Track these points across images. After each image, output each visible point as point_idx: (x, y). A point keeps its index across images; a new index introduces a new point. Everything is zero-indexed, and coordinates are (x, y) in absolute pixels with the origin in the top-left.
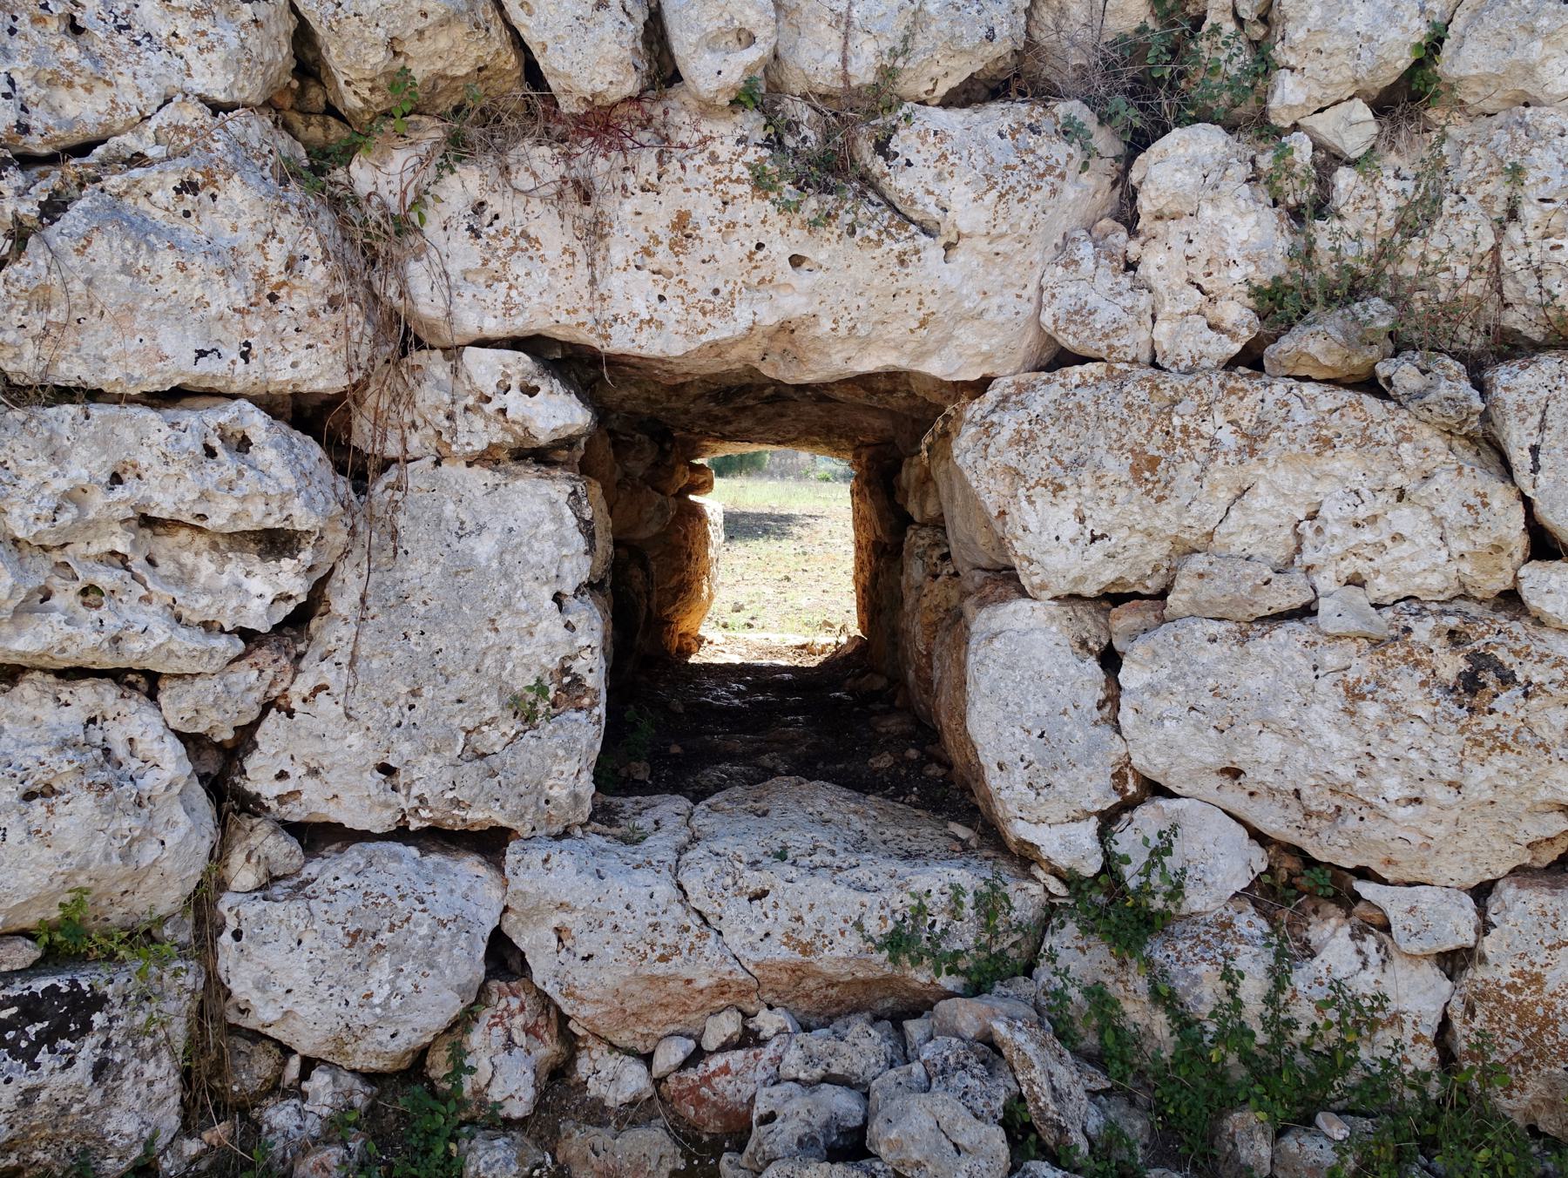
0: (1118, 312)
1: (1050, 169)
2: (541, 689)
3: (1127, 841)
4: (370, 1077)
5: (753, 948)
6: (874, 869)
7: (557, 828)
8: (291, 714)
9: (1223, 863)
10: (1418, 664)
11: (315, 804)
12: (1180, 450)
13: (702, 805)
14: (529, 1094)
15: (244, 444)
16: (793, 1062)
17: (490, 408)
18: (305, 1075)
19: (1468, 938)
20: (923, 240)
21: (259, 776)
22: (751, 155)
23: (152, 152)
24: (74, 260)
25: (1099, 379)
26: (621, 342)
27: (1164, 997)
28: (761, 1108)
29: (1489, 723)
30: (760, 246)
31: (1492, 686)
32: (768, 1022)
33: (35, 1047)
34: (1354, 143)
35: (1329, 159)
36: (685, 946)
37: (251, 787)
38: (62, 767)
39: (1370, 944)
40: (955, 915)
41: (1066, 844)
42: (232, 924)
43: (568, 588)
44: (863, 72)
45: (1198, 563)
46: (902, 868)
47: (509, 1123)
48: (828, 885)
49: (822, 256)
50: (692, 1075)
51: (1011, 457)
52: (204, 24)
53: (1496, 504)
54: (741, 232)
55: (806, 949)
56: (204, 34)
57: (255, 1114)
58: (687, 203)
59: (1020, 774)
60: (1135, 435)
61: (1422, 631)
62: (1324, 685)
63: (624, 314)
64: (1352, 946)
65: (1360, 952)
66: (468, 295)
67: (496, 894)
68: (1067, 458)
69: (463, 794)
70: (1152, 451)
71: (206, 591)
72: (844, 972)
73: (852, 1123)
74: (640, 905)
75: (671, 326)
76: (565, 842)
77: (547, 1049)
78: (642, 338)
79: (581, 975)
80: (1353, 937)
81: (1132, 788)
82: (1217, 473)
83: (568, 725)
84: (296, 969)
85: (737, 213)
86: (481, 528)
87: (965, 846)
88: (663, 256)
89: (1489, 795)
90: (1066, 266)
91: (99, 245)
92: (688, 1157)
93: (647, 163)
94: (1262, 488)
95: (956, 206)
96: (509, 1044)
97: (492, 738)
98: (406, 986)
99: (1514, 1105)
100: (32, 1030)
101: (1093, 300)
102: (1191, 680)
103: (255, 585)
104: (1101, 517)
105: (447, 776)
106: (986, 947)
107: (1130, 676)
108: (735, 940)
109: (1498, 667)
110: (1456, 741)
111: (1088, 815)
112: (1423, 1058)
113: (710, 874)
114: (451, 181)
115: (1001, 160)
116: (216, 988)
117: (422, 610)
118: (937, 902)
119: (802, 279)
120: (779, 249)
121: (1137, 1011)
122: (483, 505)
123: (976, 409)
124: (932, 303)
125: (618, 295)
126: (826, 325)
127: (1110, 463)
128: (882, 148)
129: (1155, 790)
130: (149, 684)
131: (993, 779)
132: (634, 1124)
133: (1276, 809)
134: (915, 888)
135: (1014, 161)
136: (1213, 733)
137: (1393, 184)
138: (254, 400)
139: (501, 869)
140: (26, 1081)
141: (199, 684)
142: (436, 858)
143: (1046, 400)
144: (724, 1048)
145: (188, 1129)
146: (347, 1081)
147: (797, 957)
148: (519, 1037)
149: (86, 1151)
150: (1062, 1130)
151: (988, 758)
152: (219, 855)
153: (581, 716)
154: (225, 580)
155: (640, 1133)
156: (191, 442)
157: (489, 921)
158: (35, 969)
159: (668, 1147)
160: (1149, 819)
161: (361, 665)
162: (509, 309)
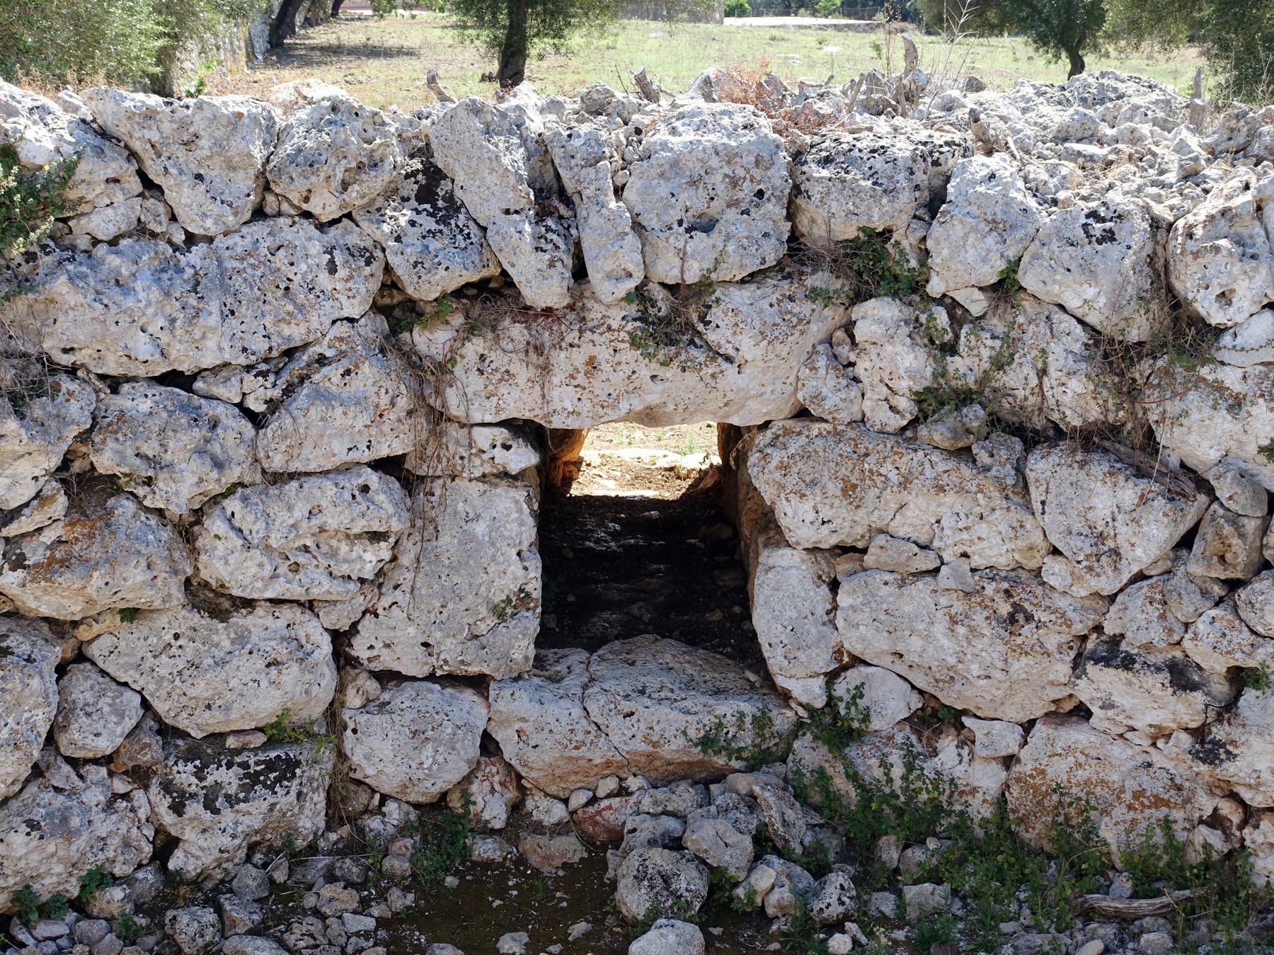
0: (838, 401)
1: (800, 321)
2: (508, 600)
3: (841, 689)
4: (417, 806)
5: (626, 743)
7: (515, 675)
8: (377, 616)
9: (892, 704)
10: (986, 607)
11: (388, 661)
12: (868, 482)
13: (595, 657)
14: (504, 817)
15: (365, 489)
16: (647, 804)
17: (485, 457)
19: (1014, 749)
20: (725, 365)
21: (359, 648)
22: (630, 327)
23: (329, 353)
24: (302, 420)
25: (829, 433)
27: (853, 777)
28: (629, 826)
29: (1019, 640)
30: (634, 372)
31: (1022, 622)
32: (633, 783)
33: (274, 784)
34: (976, 310)
36: (588, 741)
37: (354, 653)
38: (282, 652)
39: (965, 751)
40: (740, 727)
41: (805, 691)
42: (351, 725)
43: (525, 547)
44: (692, 277)
46: (711, 701)
47: (493, 832)
48: (668, 710)
49: (668, 375)
50: (591, 810)
52: (350, 285)
53: (1028, 526)
54: (624, 367)
55: (655, 745)
56: (350, 290)
57: (359, 822)
58: (594, 351)
59: (780, 651)
60: (843, 472)
61: (990, 589)
62: (940, 614)
63: (559, 409)
64: (956, 752)
65: (959, 755)
66: (477, 404)
67: (484, 711)
68: (808, 479)
69: (468, 658)
70: (854, 481)
71: (345, 561)
72: (677, 758)
73: (676, 835)
74: (564, 719)
75: (584, 414)
76: (521, 682)
77: (512, 794)
78: (569, 421)
79: (532, 756)
80: (957, 747)
81: (846, 659)
82: (887, 495)
83: (524, 621)
84: (384, 749)
86: (478, 517)
87: (752, 686)
88: (581, 379)
89: (1024, 676)
90: (811, 370)
91: (313, 411)
92: (590, 852)
93: (572, 337)
94: (912, 505)
95: (743, 348)
96: (493, 791)
97: (482, 628)
98: (440, 759)
100: (272, 776)
101: (825, 391)
102: (873, 605)
103: (368, 556)
104: (826, 513)
105: (459, 649)
106: (758, 746)
107: (843, 599)
108: (616, 739)
109: (1025, 611)
110: (1003, 648)
111: (819, 675)
112: (987, 812)
113: (602, 702)
114: (468, 344)
115: (770, 321)
116: (341, 755)
117: (447, 562)
118: (730, 720)
119: (659, 386)
121: (841, 783)
122: (478, 503)
123: (763, 439)
124: (731, 396)
125: (556, 400)
126: (671, 407)
127: (830, 485)
128: (702, 319)
129: (857, 661)
130: (310, 606)
132: (559, 834)
133: (922, 676)
134: (718, 713)
135: (778, 320)
136: (885, 634)
137: (989, 342)
139: (487, 698)
140: (271, 800)
141: (339, 606)
142: (449, 690)
143: (796, 446)
144: (608, 796)
145: (329, 828)
146: (406, 807)
147: (650, 749)
148: (497, 787)
149: (289, 835)
150: (786, 841)
151: (762, 640)
152: (341, 689)
153: (529, 614)
154: (354, 555)
155: (563, 838)
156: (347, 496)
157: (481, 725)
158: (265, 747)
159: (578, 846)
160: (853, 677)
161: (417, 592)
162: (498, 410)
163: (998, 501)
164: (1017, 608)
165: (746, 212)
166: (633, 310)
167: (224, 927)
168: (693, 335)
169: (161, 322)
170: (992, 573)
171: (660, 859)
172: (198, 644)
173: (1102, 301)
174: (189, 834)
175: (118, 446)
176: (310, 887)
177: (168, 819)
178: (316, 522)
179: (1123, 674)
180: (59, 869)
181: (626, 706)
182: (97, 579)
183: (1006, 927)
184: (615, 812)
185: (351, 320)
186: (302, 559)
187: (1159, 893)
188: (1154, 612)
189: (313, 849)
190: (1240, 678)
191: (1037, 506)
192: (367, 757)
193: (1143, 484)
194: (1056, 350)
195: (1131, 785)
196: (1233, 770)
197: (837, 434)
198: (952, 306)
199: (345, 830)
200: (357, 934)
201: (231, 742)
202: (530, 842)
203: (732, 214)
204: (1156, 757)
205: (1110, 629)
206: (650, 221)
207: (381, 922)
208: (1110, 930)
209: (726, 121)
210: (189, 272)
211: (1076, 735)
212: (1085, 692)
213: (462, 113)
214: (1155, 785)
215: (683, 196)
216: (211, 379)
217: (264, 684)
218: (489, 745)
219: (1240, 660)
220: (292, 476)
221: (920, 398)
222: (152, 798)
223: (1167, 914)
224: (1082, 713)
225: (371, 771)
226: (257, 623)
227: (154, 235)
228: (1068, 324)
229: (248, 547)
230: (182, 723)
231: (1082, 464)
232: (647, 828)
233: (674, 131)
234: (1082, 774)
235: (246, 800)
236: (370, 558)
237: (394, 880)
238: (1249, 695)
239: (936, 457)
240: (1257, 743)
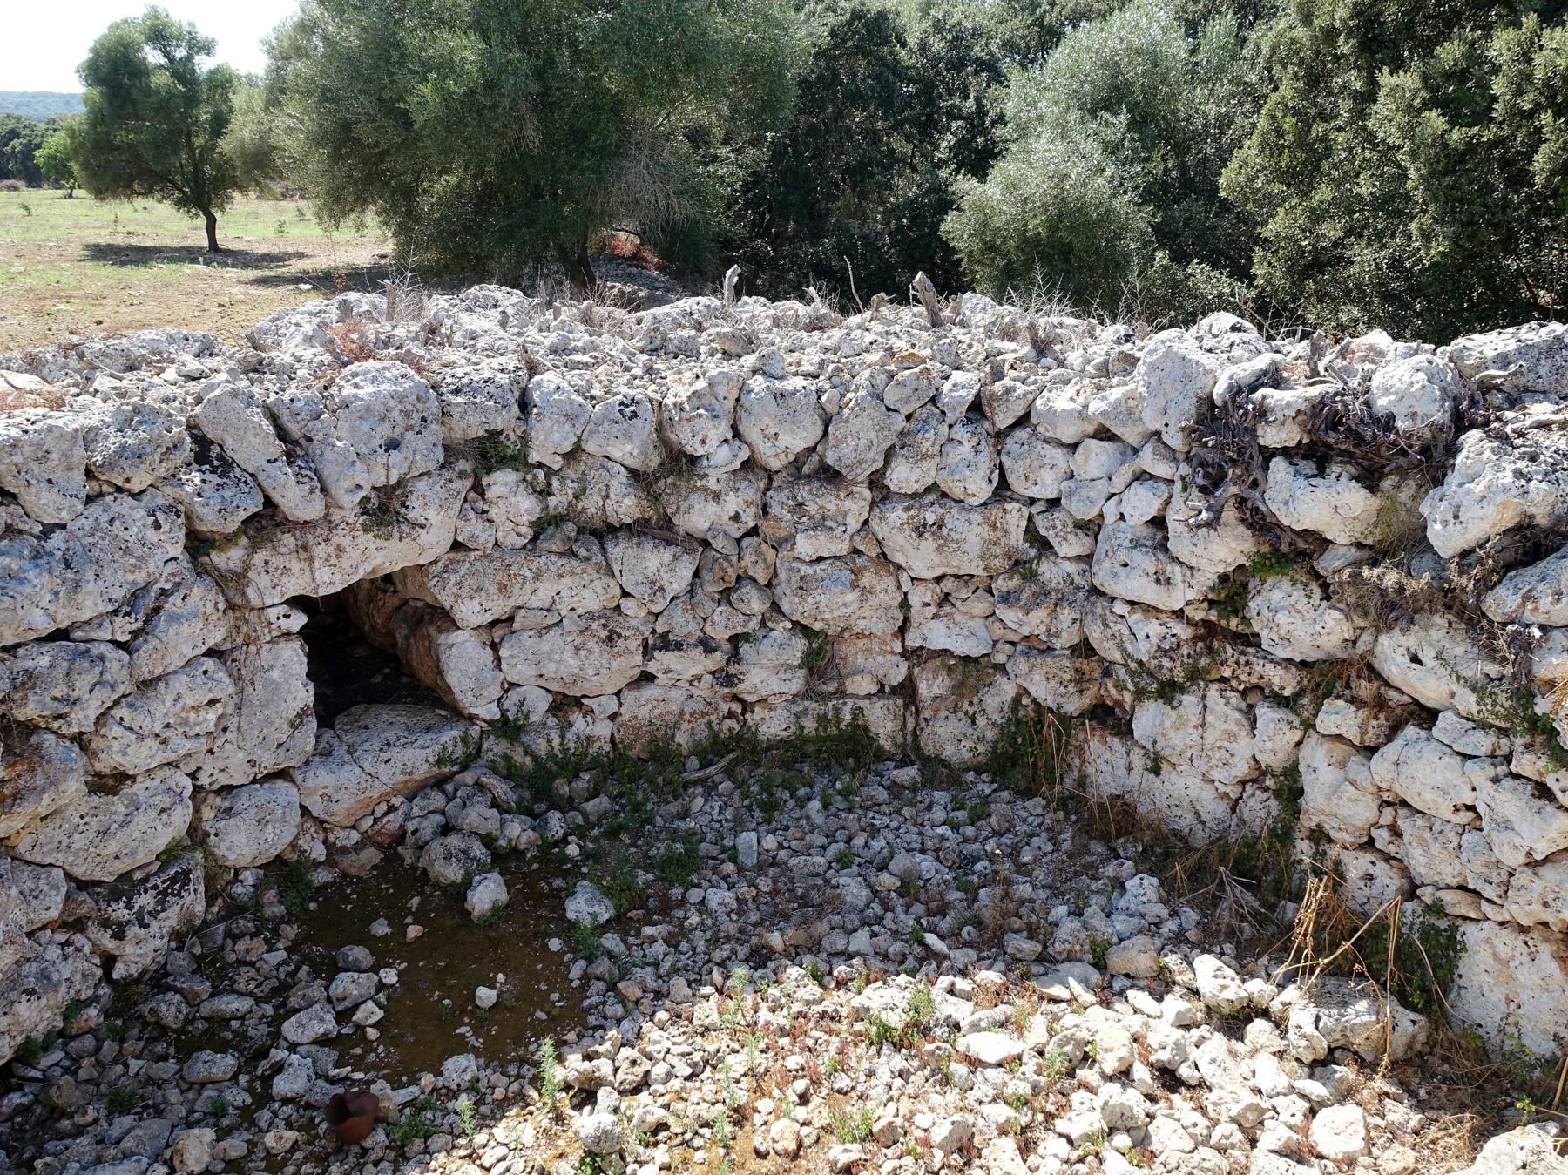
3: (507, 705)
4: (259, 867)
6: (425, 739)
11: (224, 780)
18: (236, 875)
21: (204, 780)
23: (168, 586)
26: (322, 592)
32: (396, 801)
34: (556, 467)
35: (550, 472)
42: (213, 831)
44: (393, 481)
45: (522, 613)
47: (320, 863)
50: (377, 827)
51: (455, 590)
55: (410, 774)
59: (470, 693)
61: (595, 625)
71: (196, 724)
77: (322, 837)
79: (335, 808)
85: (358, 541)
86: (271, 667)
88: (333, 561)
99: (633, 754)
104: (488, 605)
107: (503, 653)
108: (383, 778)
110: (606, 656)
112: (607, 747)
116: (209, 856)
119: (382, 553)
120: (372, 547)
121: (519, 757)
128: (403, 505)
131: (458, 696)
138: (210, 653)
139: (293, 781)
144: (385, 815)
151: (456, 690)
152: (197, 810)
157: (296, 800)
158: (161, 869)
160: (514, 695)
163: (596, 576)
164: (612, 632)
165: (419, 433)
166: (358, 510)
167: (191, 999)
168: (402, 519)
169: (48, 597)
170: (591, 616)
171: (454, 841)
172: (101, 817)
173: (635, 452)
174: (129, 949)
175: (37, 698)
176: (222, 948)
177: (110, 945)
178: (179, 705)
179: (677, 653)
180: (48, 1014)
181: (384, 756)
182: (46, 798)
183: (649, 806)
184: (393, 822)
185: (175, 559)
186: (169, 733)
187: (711, 764)
188: (689, 616)
189: (206, 924)
190: (735, 640)
191: (617, 573)
192: (229, 849)
193: (673, 548)
194: (615, 483)
195: (687, 710)
196: (741, 689)
197: (488, 556)
198: (540, 465)
199: (220, 900)
200: (279, 965)
201: (138, 875)
202: (346, 862)
203: (410, 435)
204: (695, 692)
205: (660, 630)
206: (364, 450)
207: (289, 950)
208: (699, 790)
209: (387, 374)
210: (59, 554)
211: (650, 692)
212: (652, 667)
213: (229, 399)
214: (699, 707)
215: (379, 429)
216: (86, 628)
217: (159, 827)
218: (304, 810)
219: (740, 630)
220: (159, 678)
221: (532, 524)
222: (92, 936)
223: (728, 772)
224: (647, 678)
225: (232, 857)
226: (138, 789)
227: (21, 532)
228: (618, 467)
229: (141, 738)
230: (98, 875)
231: (639, 545)
232: (428, 826)
233: (356, 386)
234: (657, 712)
235: (164, 910)
236: (211, 716)
237: (282, 920)
238: (745, 649)
239: (554, 558)
240: (754, 671)
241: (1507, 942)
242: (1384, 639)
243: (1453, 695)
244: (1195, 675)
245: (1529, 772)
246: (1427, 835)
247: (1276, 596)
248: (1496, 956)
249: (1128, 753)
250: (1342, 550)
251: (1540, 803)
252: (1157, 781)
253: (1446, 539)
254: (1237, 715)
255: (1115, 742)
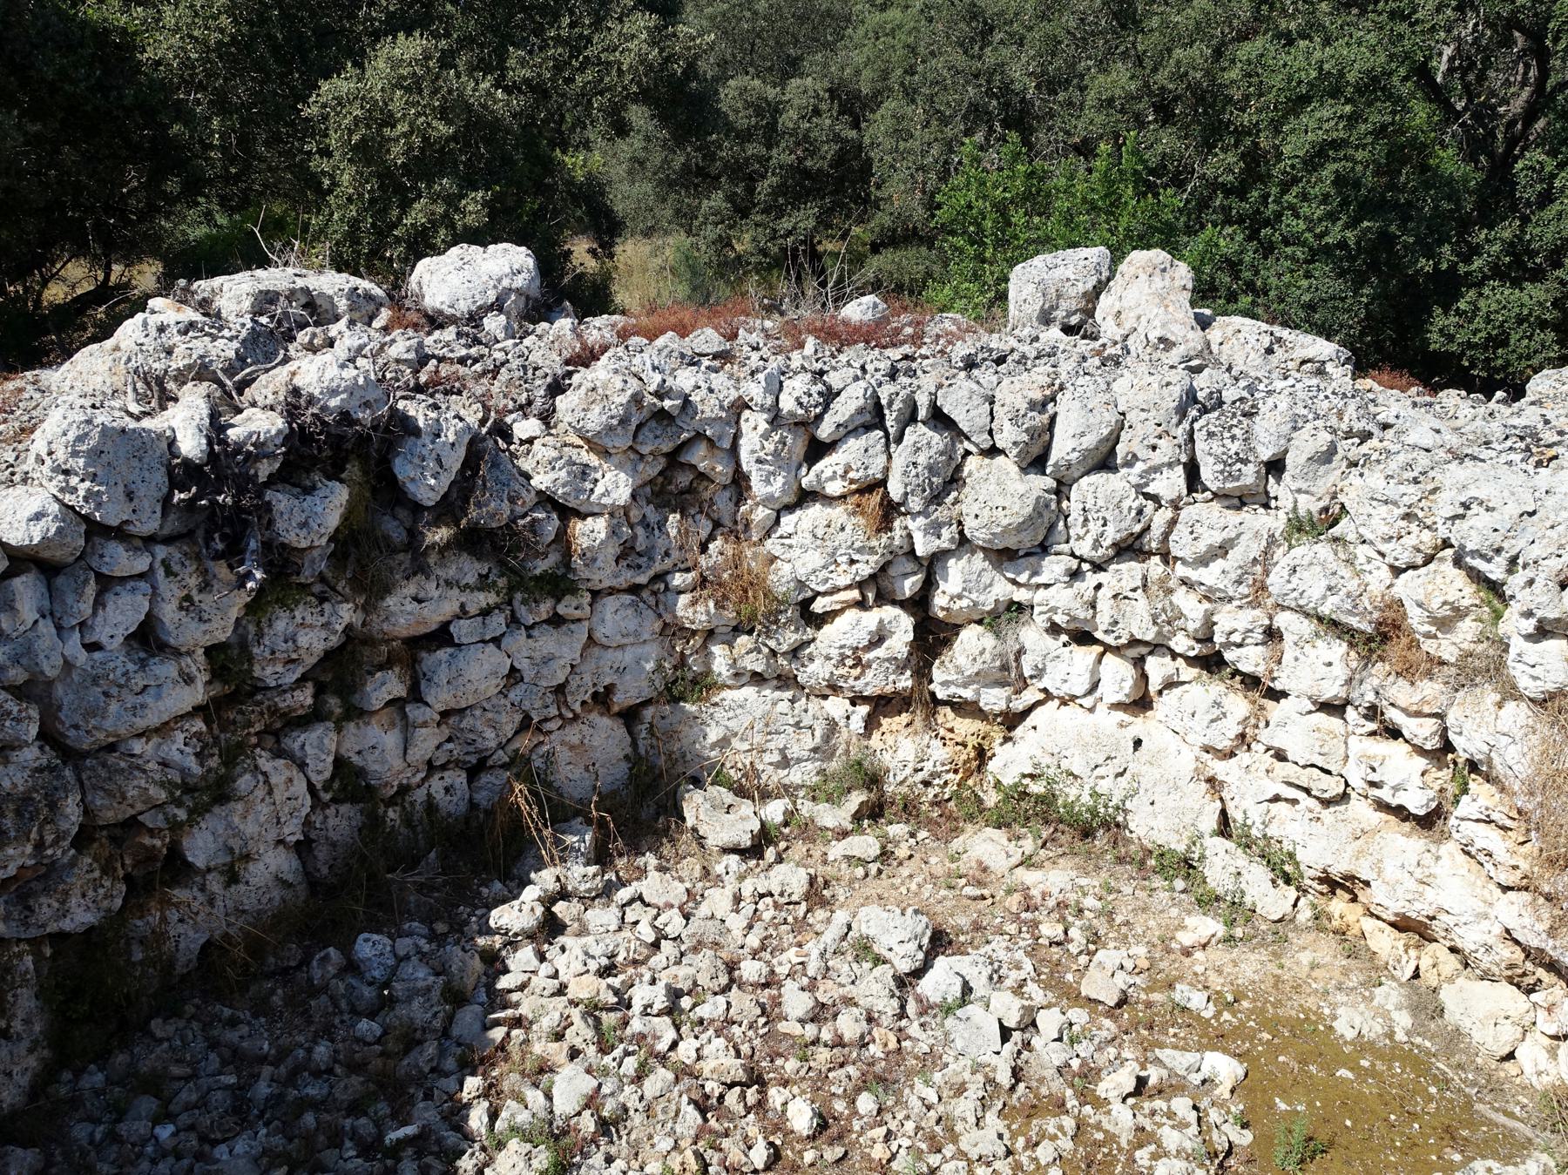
241: (573, 734)
242: (391, 601)
243: (462, 606)
244: (233, 756)
245: (544, 616)
246: (490, 715)
247: (281, 625)
248: (572, 748)
249: (203, 889)
250: (315, 553)
251: (564, 628)
252: (242, 888)
253: (429, 486)
254: (282, 761)
255: (180, 894)
